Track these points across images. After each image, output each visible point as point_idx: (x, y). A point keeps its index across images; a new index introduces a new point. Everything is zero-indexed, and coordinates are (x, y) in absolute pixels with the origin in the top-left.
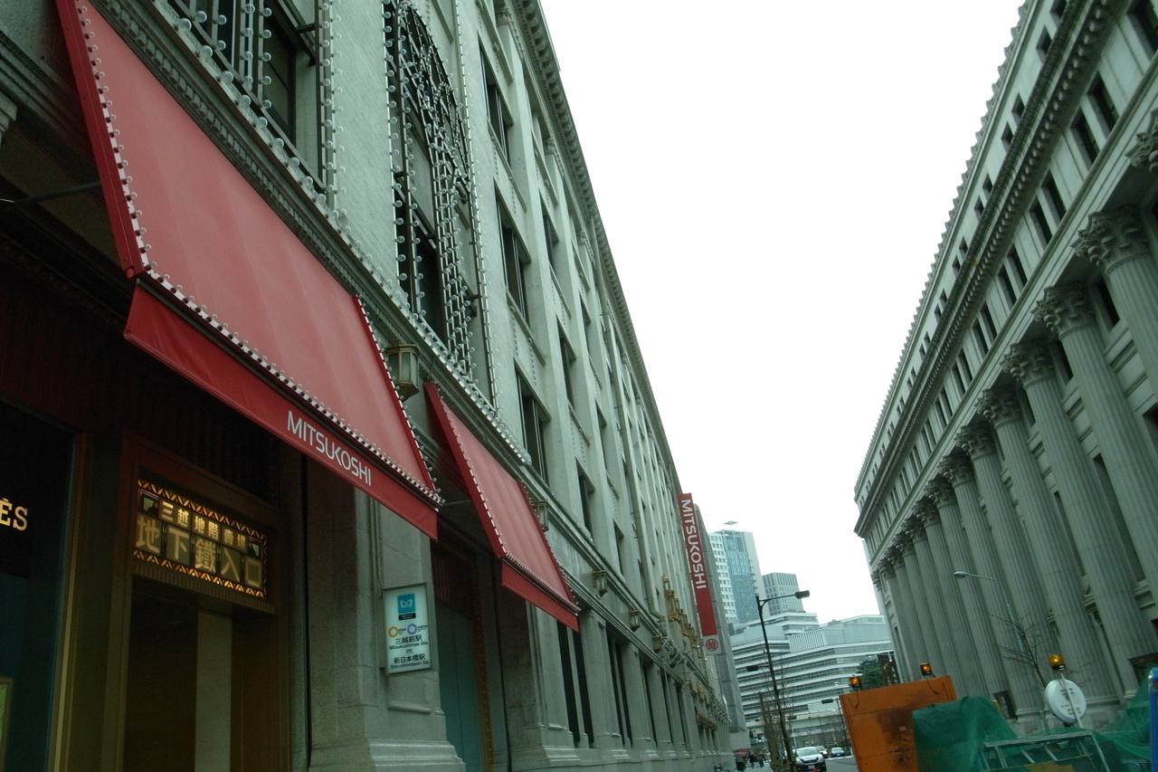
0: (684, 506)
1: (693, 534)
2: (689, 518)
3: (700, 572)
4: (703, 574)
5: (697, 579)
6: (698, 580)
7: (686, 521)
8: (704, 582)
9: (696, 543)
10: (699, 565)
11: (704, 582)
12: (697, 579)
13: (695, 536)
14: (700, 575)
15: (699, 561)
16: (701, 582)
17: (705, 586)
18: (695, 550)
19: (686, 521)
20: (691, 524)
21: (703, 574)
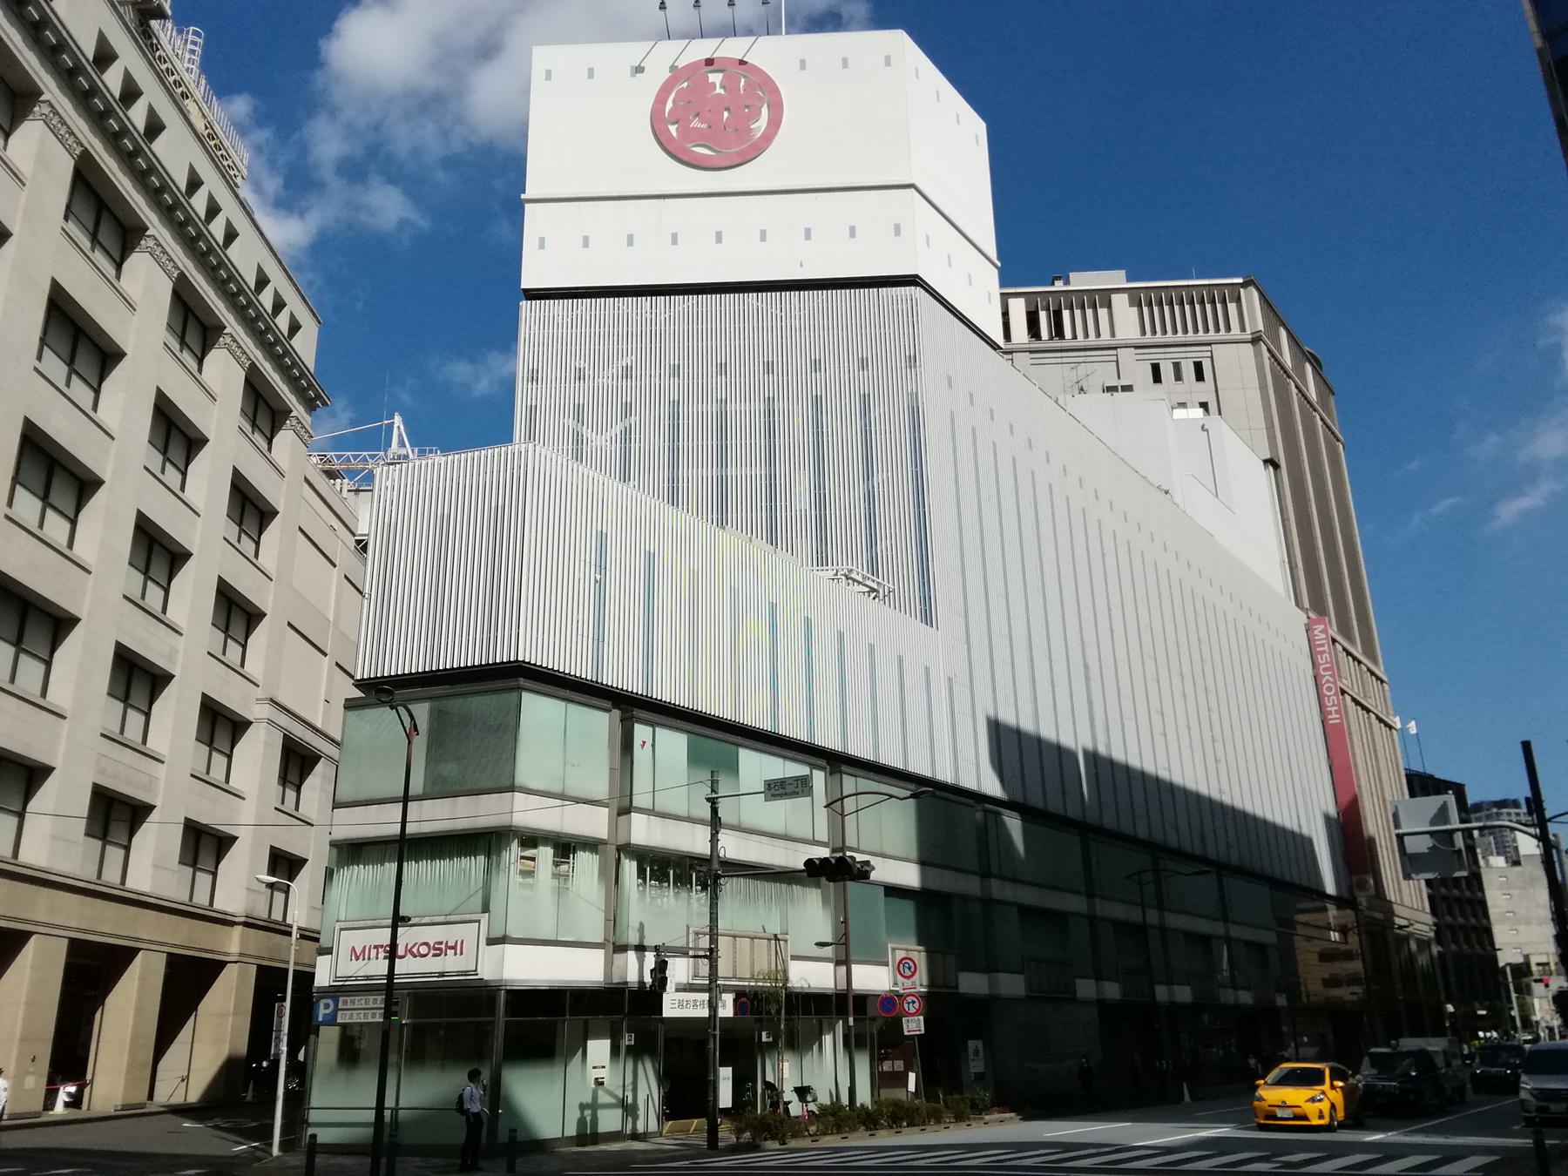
0: (1316, 632)
1: (1327, 662)
2: (1323, 645)
3: (1334, 705)
4: (1336, 708)
5: (1330, 713)
6: (1331, 714)
7: (1318, 649)
8: (1338, 716)
9: (1330, 673)
10: (1331, 698)
11: (1338, 716)
12: (1330, 713)
13: (1329, 665)
14: (1333, 709)
15: (1333, 692)
16: (1334, 716)
17: (1338, 721)
18: (1328, 681)
19: (1318, 649)
20: (1324, 651)
21: (1336, 708)
